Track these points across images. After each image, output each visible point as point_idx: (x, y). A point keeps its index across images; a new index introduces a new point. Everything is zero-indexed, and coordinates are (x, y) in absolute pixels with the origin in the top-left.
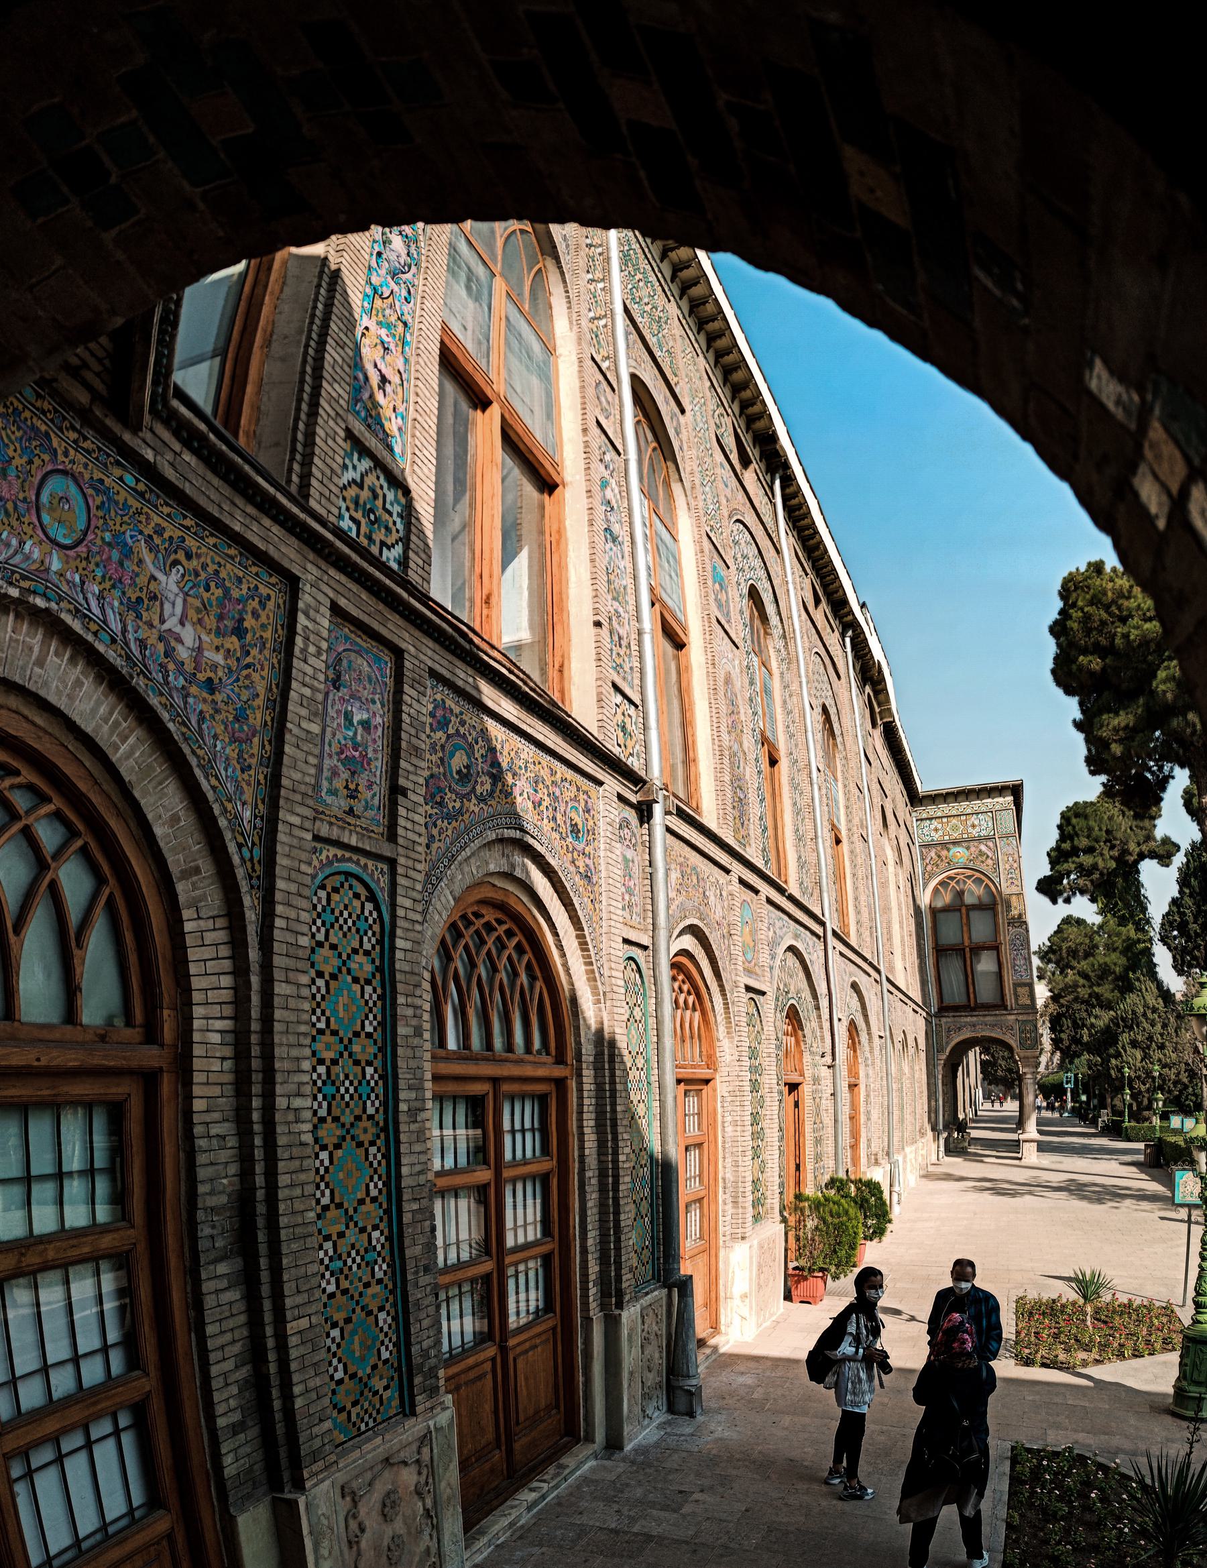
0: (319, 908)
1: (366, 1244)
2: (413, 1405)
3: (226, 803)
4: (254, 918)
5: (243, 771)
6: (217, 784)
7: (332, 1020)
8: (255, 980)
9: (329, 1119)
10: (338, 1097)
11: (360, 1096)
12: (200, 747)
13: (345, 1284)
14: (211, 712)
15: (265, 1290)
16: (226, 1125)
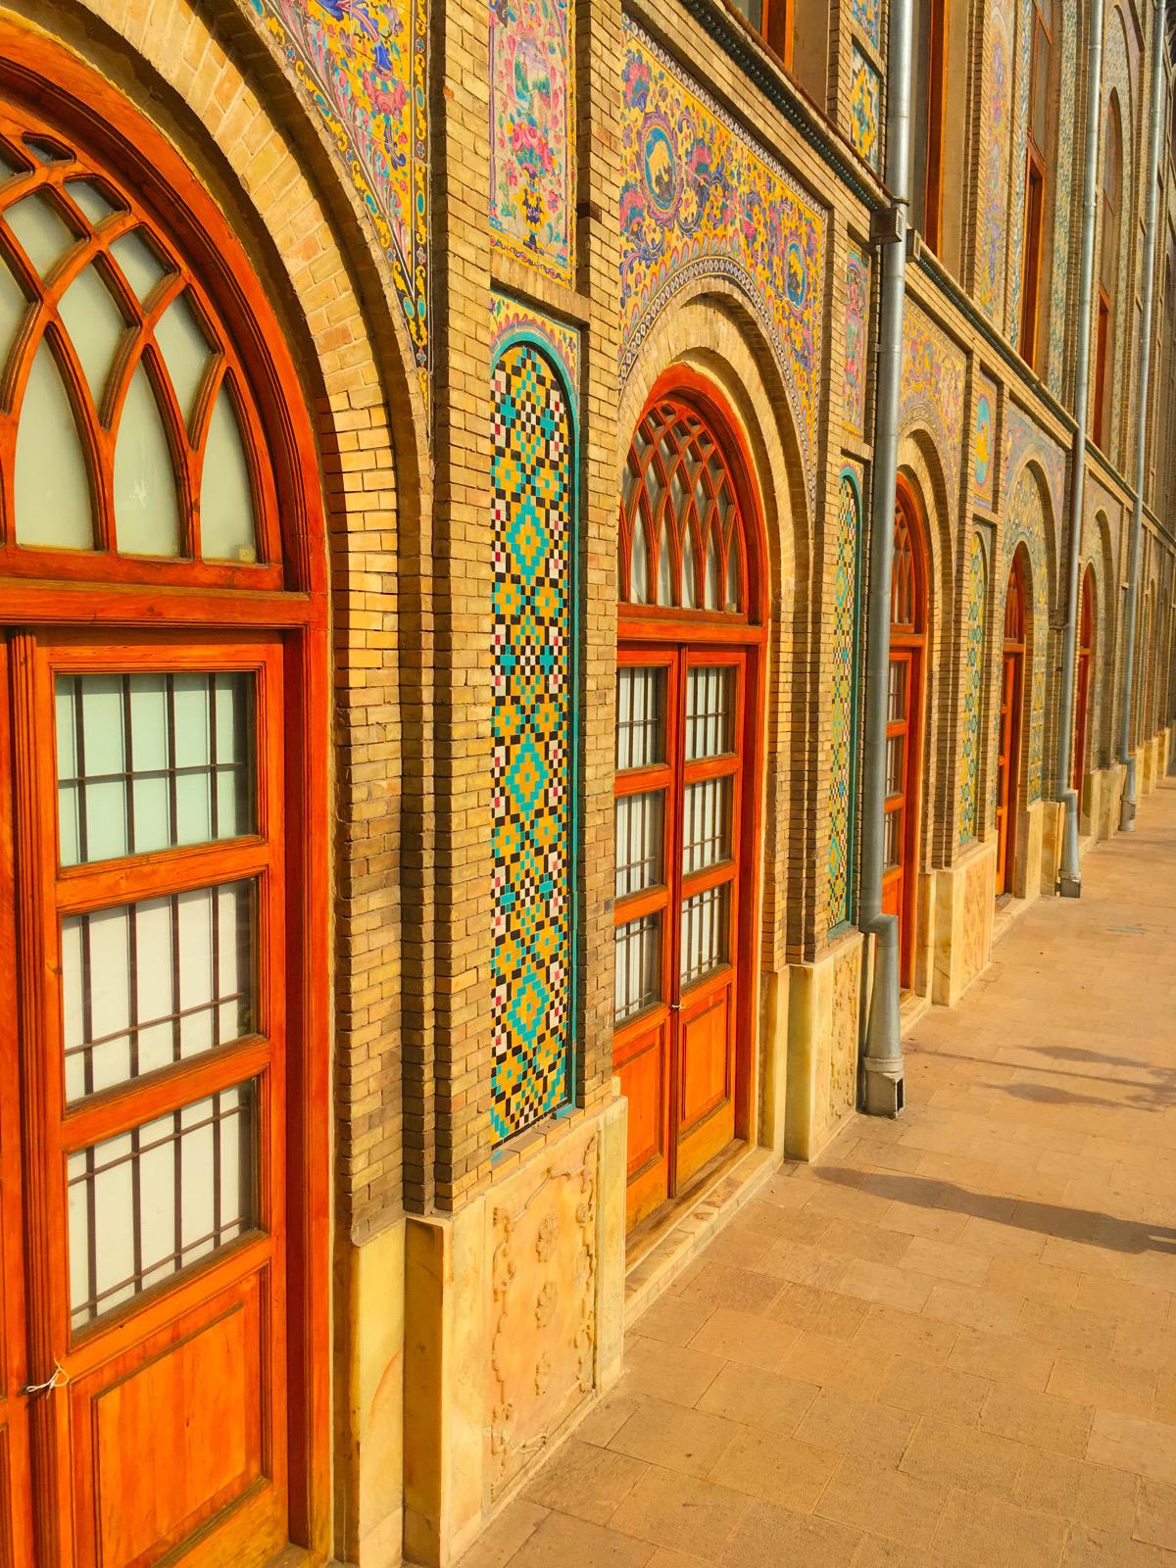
1: (541, 871)
2: (581, 1093)
3: (378, 221)
4: (422, 411)
6: (364, 187)
7: (513, 557)
8: (426, 502)
9: (508, 699)
10: (518, 669)
11: (542, 669)
12: (334, 118)
13: (516, 925)
14: (343, 54)
15: (428, 931)
16: (389, 708)
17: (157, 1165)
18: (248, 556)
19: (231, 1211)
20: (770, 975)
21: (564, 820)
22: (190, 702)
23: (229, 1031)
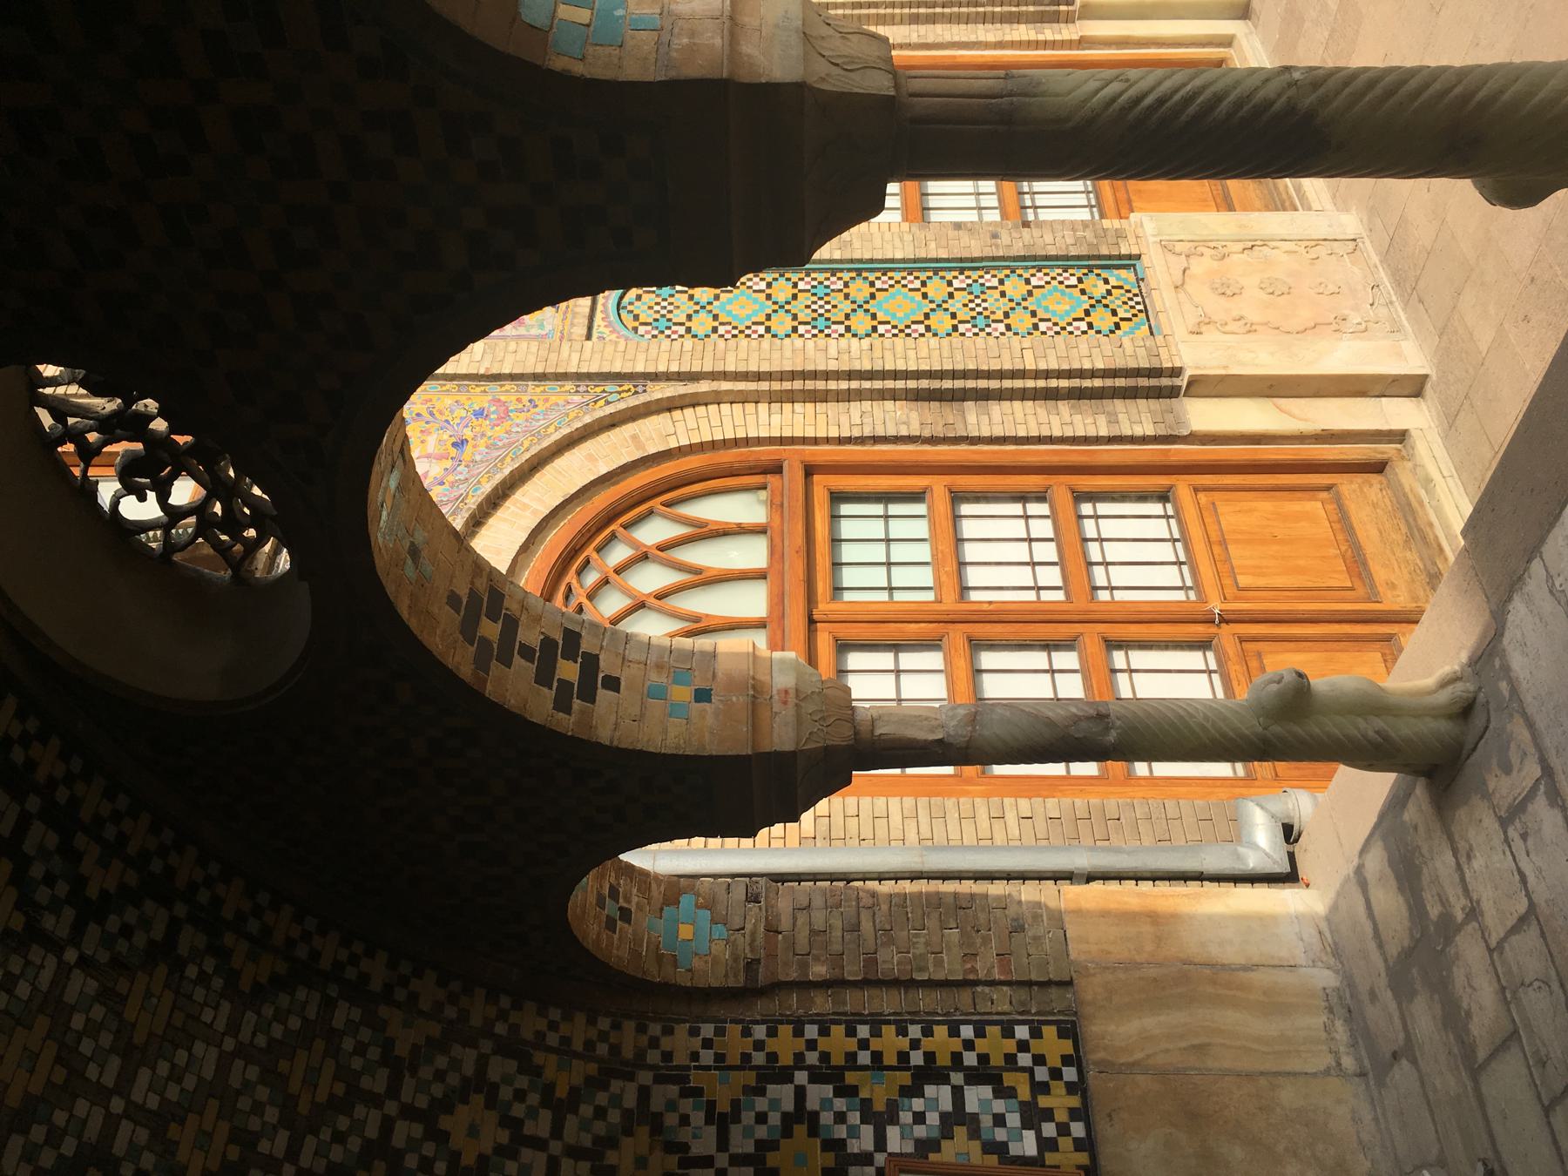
0: (656, 332)
1: (965, 293)
2: (1130, 257)
3: (570, 418)
4: (672, 389)
5: (536, 406)
6: (553, 427)
7: (754, 320)
8: (726, 386)
9: (847, 323)
10: (827, 315)
11: (827, 295)
12: (522, 445)
13: (1000, 315)
14: (485, 439)
15: (994, 384)
16: (852, 409)
17: (1114, 552)
18: (763, 495)
19: (1156, 508)
20: (1083, 42)
21: (931, 274)
22: (847, 529)
23: (1043, 509)
